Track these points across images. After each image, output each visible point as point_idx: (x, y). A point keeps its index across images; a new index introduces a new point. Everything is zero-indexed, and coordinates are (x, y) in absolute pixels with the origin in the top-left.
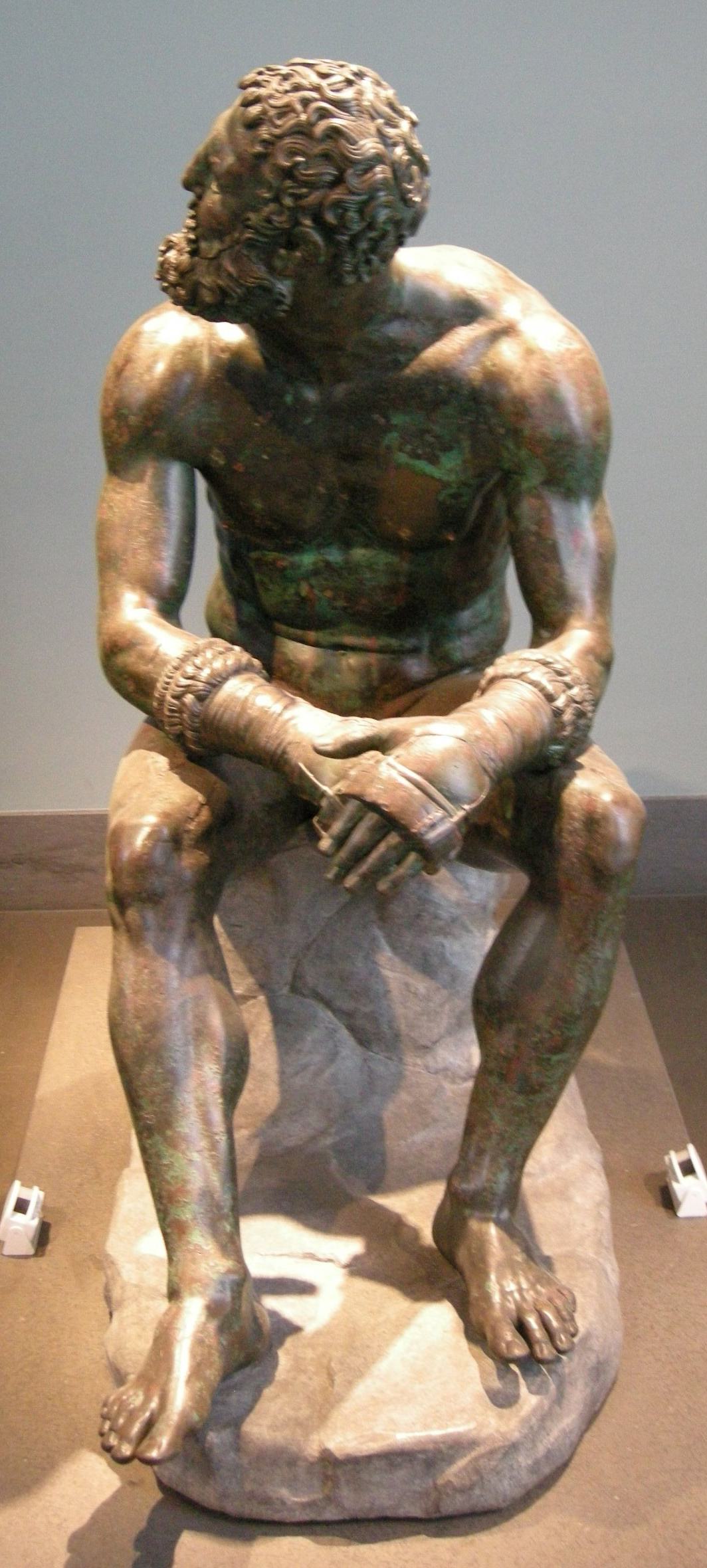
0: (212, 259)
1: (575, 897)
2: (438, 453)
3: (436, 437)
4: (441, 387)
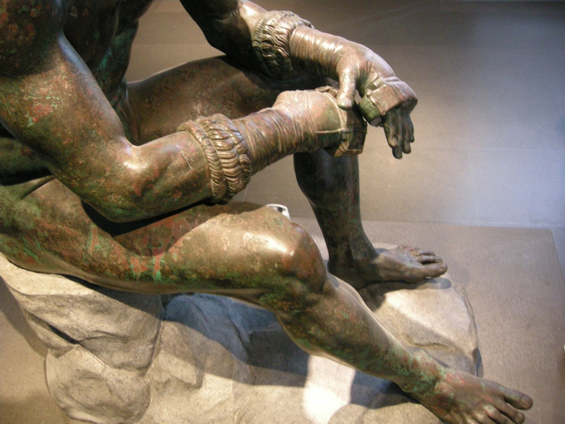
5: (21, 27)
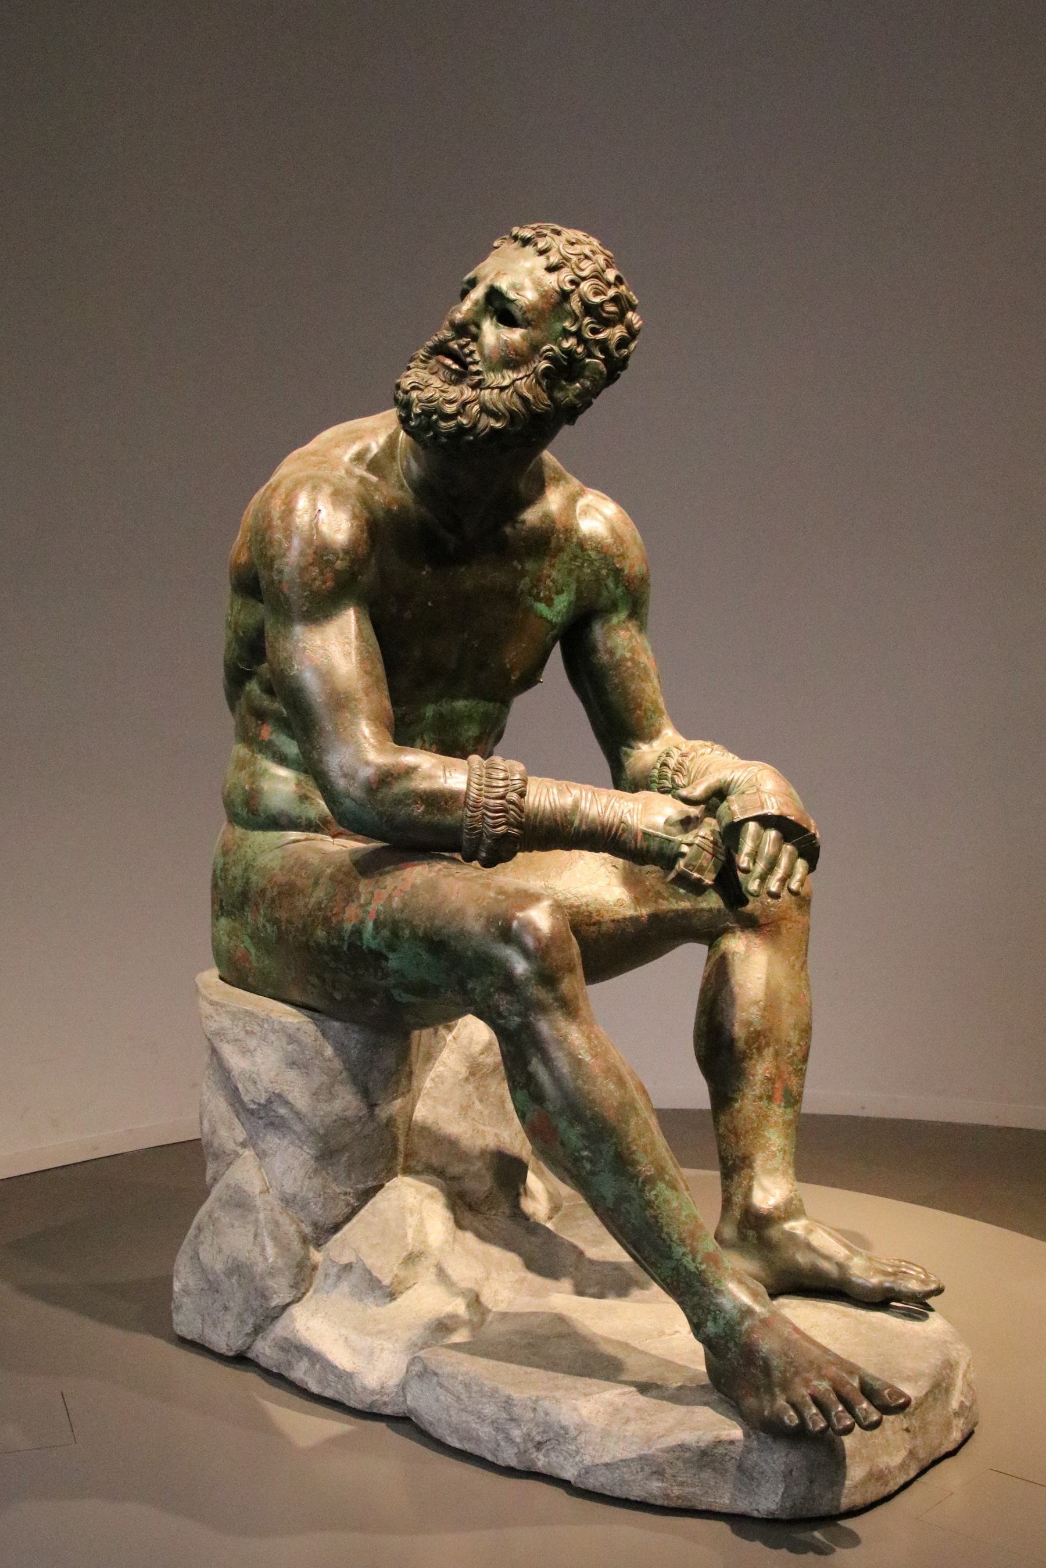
0: (502, 389)
1: (789, 925)
2: (553, 596)
3: (553, 581)
4: (561, 536)
5: (322, 573)
